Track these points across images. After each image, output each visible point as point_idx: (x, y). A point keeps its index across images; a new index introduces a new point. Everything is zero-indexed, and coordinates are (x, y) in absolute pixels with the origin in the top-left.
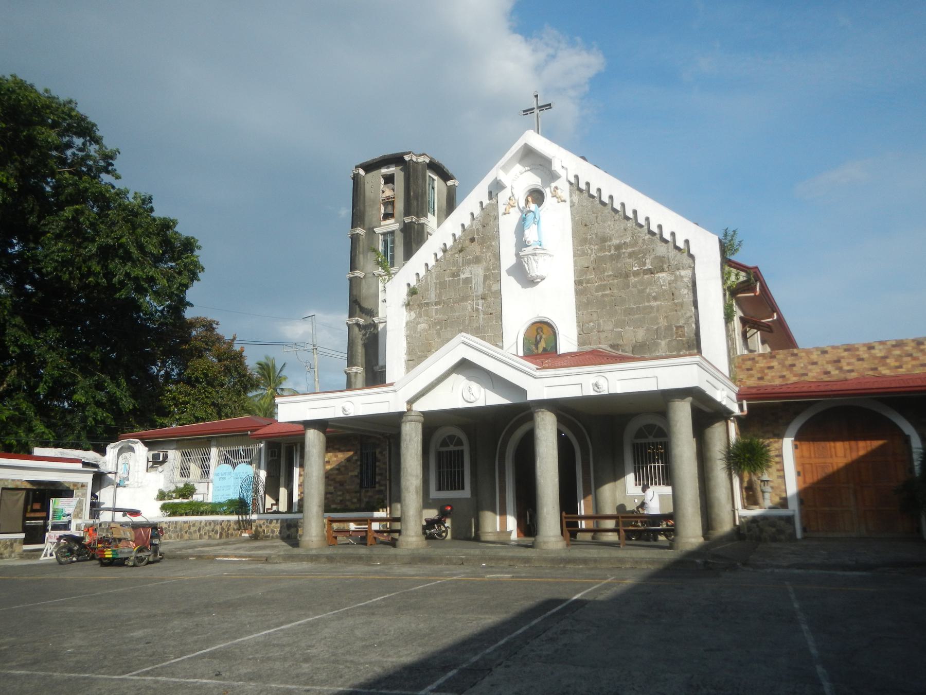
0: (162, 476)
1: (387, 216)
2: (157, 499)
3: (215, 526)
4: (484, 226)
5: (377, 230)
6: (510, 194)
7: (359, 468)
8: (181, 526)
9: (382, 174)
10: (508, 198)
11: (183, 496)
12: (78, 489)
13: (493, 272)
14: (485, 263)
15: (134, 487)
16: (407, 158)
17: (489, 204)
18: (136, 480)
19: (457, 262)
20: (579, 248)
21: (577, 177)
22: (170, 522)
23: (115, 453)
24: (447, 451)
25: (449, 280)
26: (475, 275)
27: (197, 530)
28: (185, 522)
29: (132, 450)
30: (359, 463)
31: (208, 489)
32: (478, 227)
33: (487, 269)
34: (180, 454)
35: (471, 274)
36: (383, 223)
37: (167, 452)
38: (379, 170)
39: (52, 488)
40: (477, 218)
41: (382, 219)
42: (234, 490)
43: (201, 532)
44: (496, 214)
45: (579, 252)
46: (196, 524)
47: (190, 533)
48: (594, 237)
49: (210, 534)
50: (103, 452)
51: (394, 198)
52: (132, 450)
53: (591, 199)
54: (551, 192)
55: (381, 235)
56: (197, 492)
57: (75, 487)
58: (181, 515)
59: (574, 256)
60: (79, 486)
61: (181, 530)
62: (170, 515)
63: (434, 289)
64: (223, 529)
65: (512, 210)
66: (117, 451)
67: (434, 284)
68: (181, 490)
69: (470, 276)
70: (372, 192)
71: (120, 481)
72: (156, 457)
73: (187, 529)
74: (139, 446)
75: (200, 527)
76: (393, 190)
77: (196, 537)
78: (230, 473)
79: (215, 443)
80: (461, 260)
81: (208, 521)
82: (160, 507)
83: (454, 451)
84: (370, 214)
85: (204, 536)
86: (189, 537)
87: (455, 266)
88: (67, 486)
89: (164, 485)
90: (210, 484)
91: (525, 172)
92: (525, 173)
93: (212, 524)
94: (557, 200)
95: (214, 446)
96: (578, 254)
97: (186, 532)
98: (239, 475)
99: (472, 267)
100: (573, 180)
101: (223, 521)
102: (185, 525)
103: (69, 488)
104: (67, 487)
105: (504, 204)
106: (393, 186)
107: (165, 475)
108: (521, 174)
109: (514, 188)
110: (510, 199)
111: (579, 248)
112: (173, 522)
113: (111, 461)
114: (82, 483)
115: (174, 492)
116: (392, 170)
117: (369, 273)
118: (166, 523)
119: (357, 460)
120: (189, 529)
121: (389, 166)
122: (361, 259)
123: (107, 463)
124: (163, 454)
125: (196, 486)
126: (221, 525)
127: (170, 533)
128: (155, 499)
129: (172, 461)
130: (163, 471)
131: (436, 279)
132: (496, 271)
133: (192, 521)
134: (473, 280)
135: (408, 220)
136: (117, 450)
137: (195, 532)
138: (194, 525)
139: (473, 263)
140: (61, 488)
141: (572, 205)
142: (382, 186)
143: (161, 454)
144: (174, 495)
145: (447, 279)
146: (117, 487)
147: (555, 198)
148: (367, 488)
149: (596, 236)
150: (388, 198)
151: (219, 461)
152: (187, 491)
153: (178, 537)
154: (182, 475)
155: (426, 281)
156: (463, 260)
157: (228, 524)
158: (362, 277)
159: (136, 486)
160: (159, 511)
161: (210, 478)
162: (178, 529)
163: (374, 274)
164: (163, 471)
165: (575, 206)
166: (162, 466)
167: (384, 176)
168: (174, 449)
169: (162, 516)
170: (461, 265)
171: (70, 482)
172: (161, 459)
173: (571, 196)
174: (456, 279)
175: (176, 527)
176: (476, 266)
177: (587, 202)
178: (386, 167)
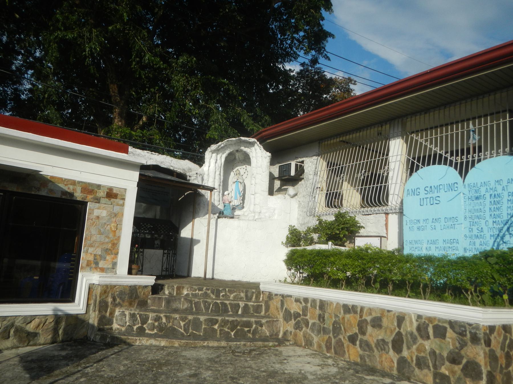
0: (294, 203)
2: (286, 243)
3: (463, 345)
8: (336, 316)
11: (335, 238)
12: (97, 200)
15: (248, 220)
18: (252, 209)
22: (306, 300)
23: (219, 161)
27: (389, 339)
28: (348, 309)
29: (246, 160)
31: (387, 229)
34: (325, 164)
37: (302, 162)
39: (13, 188)
42: (471, 230)
43: (405, 353)
46: (385, 322)
47: (366, 346)
49: (444, 370)
50: (199, 161)
52: (246, 160)
56: (362, 232)
57: (90, 197)
58: (335, 284)
60: (101, 194)
61: (337, 329)
62: (306, 282)
64: (492, 357)
66: (223, 160)
68: (330, 226)
71: (225, 206)
72: (284, 171)
73: (356, 330)
74: (256, 150)
75: (399, 334)
77: (386, 365)
78: (452, 187)
79: (400, 130)
81: (431, 319)
82: (285, 258)
85: (417, 371)
86: (362, 357)
88: (66, 188)
89: (298, 219)
90: (390, 215)
93: (450, 333)
95: (394, 137)
97: (352, 339)
98: (483, 190)
101: (492, 329)
102: (348, 316)
103: (71, 195)
104: (65, 193)
107: (300, 204)
112: (314, 301)
113: (212, 175)
114: (111, 189)
115: (315, 230)
118: (297, 300)
120: (364, 333)
123: (205, 177)
124: (296, 165)
125: (360, 219)
126: (488, 343)
127: (308, 331)
128: (282, 242)
129: (311, 177)
130: (296, 195)
133: (370, 309)
136: (222, 157)
137: (382, 344)
138: (377, 323)
140: (43, 193)
143: (293, 164)
144: (315, 236)
146: (219, 217)
151: (413, 163)
152: (342, 229)
153: (328, 348)
154: (330, 204)
157: (505, 338)
159: (251, 218)
160: (284, 267)
161: (390, 203)
162: (329, 324)
164: (296, 195)
166: (296, 187)
168: (316, 156)
169: (289, 280)
171: (74, 183)
172: (293, 173)
175: (321, 318)
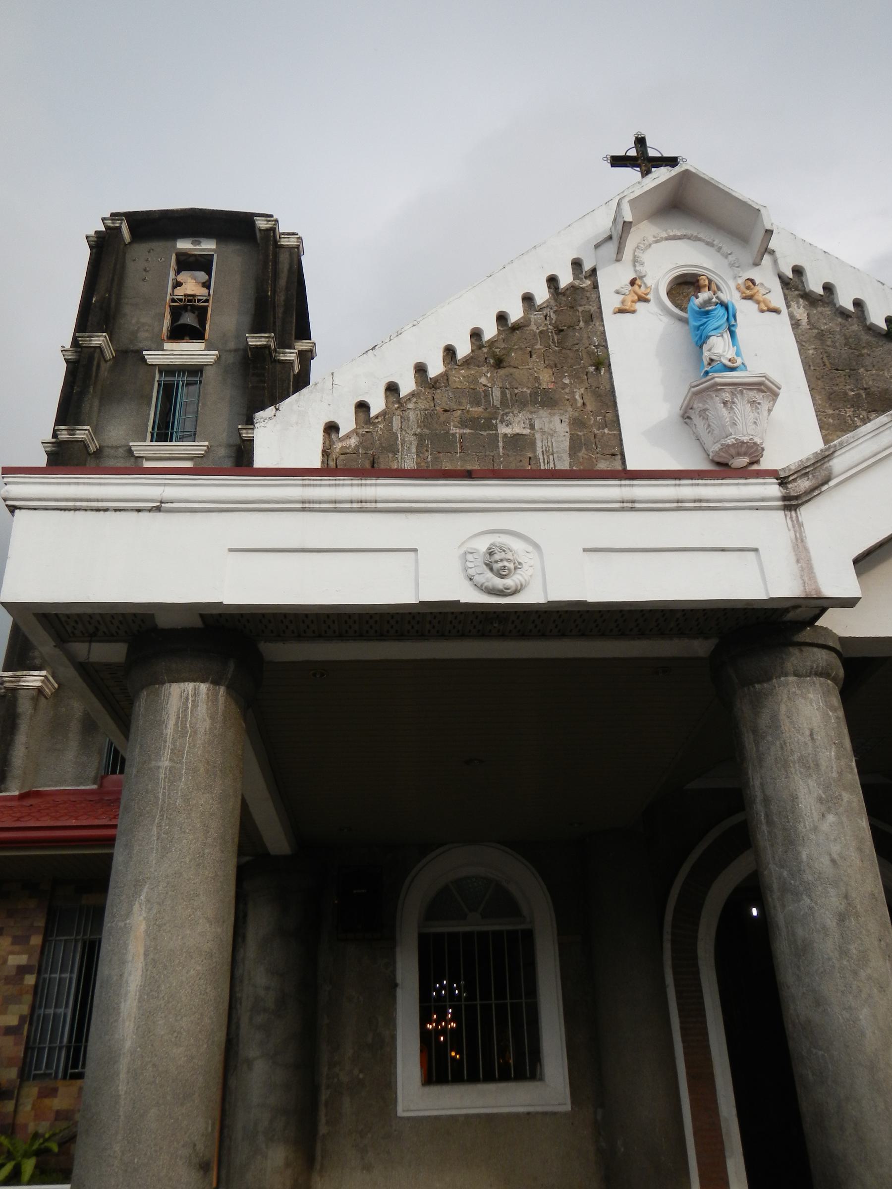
1: (179, 333)
4: (562, 330)
5: (153, 357)
6: (633, 276)
7: (28, 998)
9: (176, 251)
10: (629, 280)
13: (596, 432)
14: (570, 409)
16: (261, 224)
17: (572, 286)
19: (486, 394)
20: (831, 412)
21: (798, 271)
24: (453, 936)
25: (461, 436)
26: (543, 433)
30: (30, 980)
32: (541, 328)
33: (577, 423)
35: (532, 427)
36: (168, 346)
38: (169, 244)
40: (541, 309)
41: (165, 338)
44: (593, 309)
45: (831, 420)
48: (864, 396)
51: (207, 301)
53: (840, 320)
54: (738, 288)
55: (160, 372)
59: (821, 428)
63: (414, 450)
65: (639, 306)
67: (413, 438)
69: (527, 431)
70: (144, 280)
76: (206, 285)
80: (497, 394)
83: (483, 935)
84: (134, 321)
87: (478, 404)
91: (667, 239)
92: (664, 243)
94: (756, 306)
96: (828, 424)
99: (531, 413)
100: (790, 274)
105: (617, 292)
106: (207, 277)
108: (657, 242)
109: (642, 264)
110: (633, 283)
111: (831, 412)
116: (208, 246)
117: (112, 447)
119: (22, 970)
121: (201, 240)
122: (91, 404)
131: (419, 426)
132: (606, 431)
134: (539, 444)
135: (255, 341)
139: (534, 402)
141: (796, 324)
142: (172, 275)
145: (454, 430)
147: (749, 302)
148: (45, 1076)
149: (868, 394)
150: (191, 298)
155: (389, 427)
156: (503, 394)
158: (92, 449)
163: (130, 451)
165: (801, 327)
167: (182, 258)
170: (497, 403)
173: (788, 306)
174: (485, 433)
176: (544, 413)
177: (833, 325)
178: (191, 240)
